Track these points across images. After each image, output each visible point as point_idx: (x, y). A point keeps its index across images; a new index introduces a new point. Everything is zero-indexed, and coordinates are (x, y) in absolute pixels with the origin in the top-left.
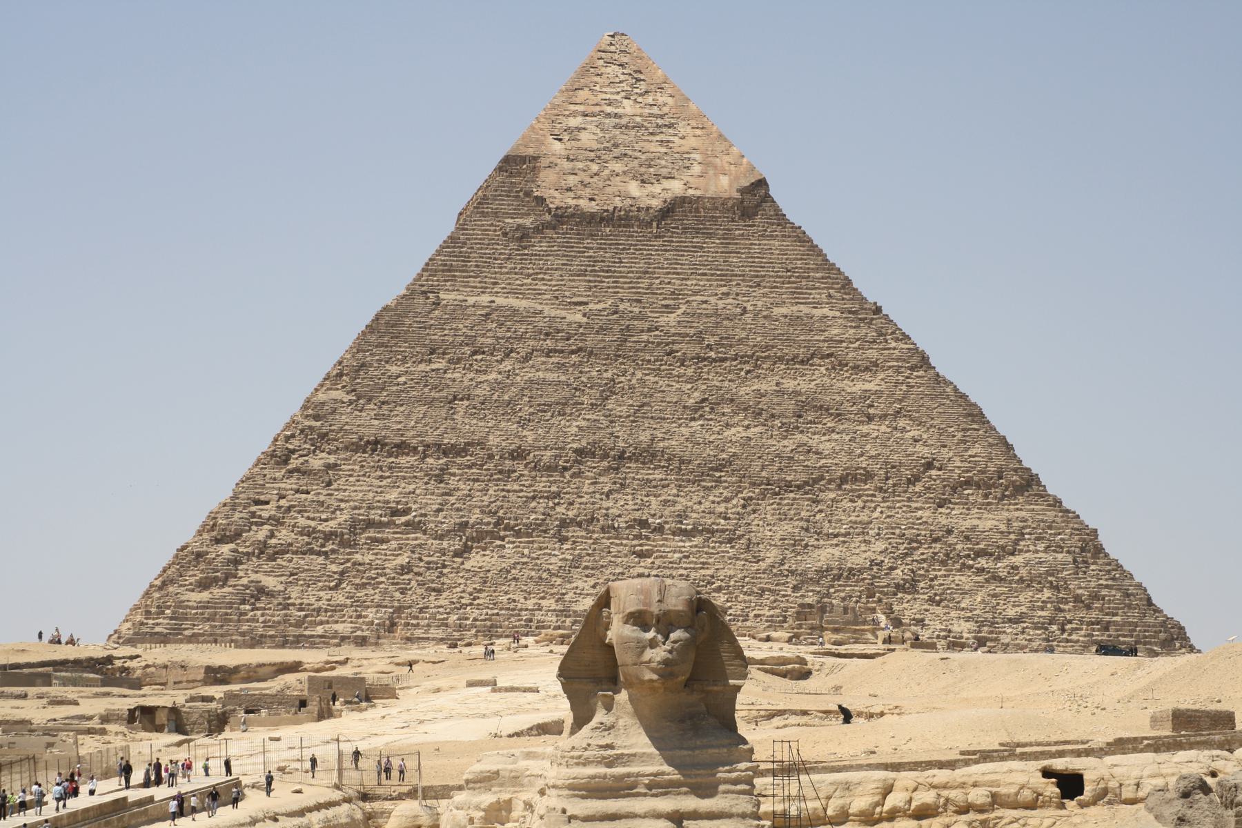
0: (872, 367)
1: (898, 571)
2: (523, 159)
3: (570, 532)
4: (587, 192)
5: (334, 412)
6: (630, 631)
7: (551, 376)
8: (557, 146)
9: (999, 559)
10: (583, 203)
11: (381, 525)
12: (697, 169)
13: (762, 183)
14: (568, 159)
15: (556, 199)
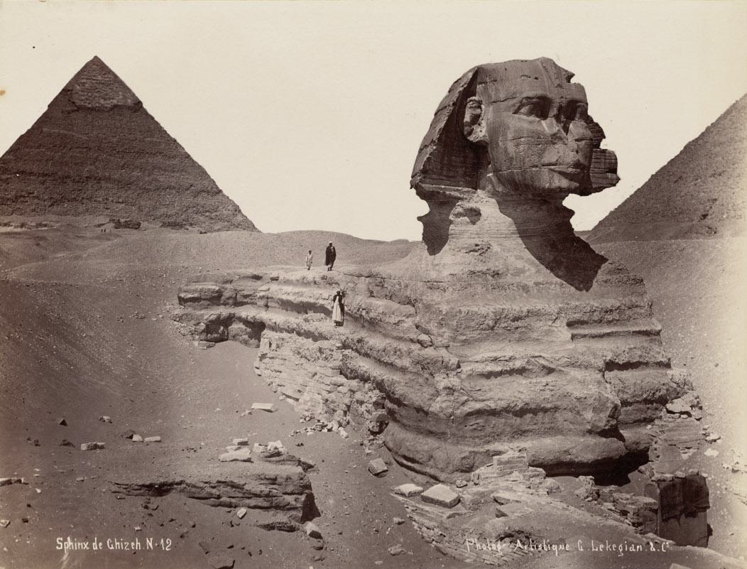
0: (174, 157)
1: (183, 216)
2: (69, 91)
3: (84, 201)
4: (88, 101)
5: (9, 162)
6: (524, 122)
7: (78, 155)
8: (78, 87)
9: (212, 213)
10: (86, 104)
11: (24, 197)
12: (121, 97)
13: (139, 103)
14: (82, 91)
15: (78, 103)
